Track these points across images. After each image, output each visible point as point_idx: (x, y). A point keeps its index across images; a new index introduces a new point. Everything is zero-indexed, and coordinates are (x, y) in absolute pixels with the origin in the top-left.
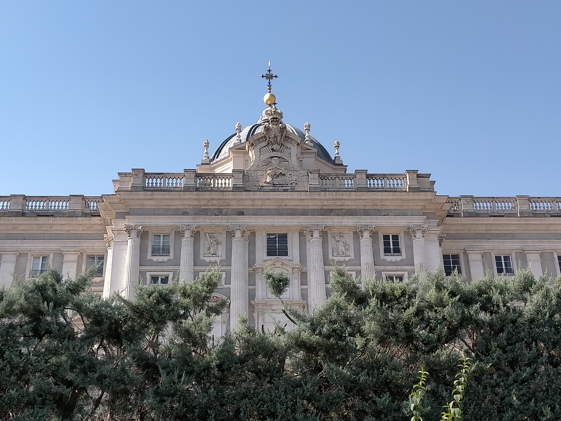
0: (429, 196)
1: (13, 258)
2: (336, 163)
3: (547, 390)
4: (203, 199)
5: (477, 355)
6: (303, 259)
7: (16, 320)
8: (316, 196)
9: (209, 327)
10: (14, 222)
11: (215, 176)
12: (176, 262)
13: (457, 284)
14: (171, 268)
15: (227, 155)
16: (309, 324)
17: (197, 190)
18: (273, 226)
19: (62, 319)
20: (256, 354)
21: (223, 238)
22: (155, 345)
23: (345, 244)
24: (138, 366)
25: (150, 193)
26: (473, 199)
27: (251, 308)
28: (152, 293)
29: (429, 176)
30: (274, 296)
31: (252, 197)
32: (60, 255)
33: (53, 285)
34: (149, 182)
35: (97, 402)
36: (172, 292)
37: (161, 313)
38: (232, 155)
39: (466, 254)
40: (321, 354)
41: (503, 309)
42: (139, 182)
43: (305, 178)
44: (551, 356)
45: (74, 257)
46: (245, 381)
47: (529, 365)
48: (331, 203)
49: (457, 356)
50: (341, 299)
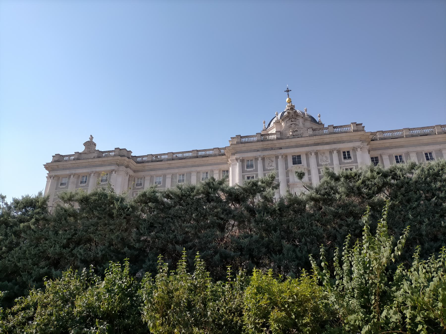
0: (362, 133)
1: (195, 174)
2: (319, 123)
3: (426, 211)
4: (265, 144)
6: (308, 165)
7: (201, 196)
8: (312, 138)
9: (274, 194)
10: (194, 160)
11: (269, 135)
13: (380, 169)
14: (254, 173)
15: (273, 126)
16: (315, 190)
17: (262, 141)
18: (294, 153)
19: (217, 195)
20: (294, 204)
22: (253, 203)
23: (326, 157)
24: (247, 211)
25: (243, 144)
26: (383, 132)
29: (361, 124)
30: (299, 180)
31: (284, 142)
33: (212, 182)
34: (243, 140)
35: (233, 226)
38: (275, 125)
40: (321, 202)
41: (402, 178)
42: (239, 140)
44: (426, 197)
45: (217, 172)
46: (290, 215)
47: (416, 201)
49: (382, 199)
50: (328, 179)
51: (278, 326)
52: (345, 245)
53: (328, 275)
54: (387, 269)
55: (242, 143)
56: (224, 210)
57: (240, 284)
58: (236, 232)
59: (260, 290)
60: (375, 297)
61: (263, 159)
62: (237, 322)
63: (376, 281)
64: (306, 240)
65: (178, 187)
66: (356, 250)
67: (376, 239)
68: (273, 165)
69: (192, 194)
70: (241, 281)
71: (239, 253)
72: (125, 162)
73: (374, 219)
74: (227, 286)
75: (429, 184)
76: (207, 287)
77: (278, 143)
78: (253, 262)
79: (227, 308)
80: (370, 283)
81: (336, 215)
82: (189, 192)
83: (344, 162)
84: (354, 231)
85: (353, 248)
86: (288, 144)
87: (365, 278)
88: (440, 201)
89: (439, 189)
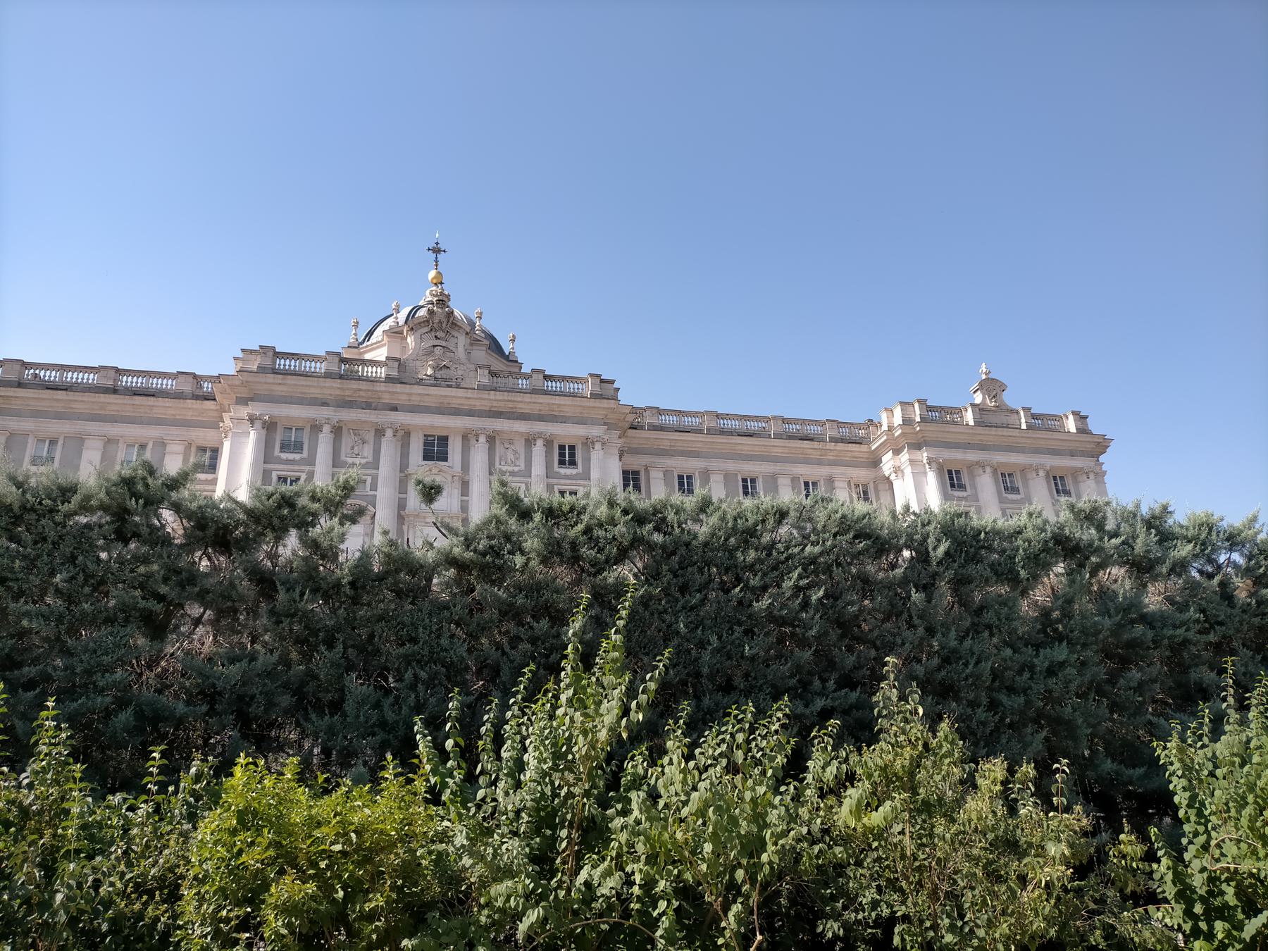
0: (612, 404)
2: (510, 359)
4: (348, 389)
5: (646, 578)
6: (465, 466)
7: (95, 519)
8: (485, 395)
9: (342, 538)
11: (364, 363)
12: (311, 461)
15: (380, 339)
16: (462, 539)
17: (341, 377)
18: (432, 427)
19: (156, 522)
20: (397, 571)
21: (370, 437)
22: (273, 556)
23: (515, 452)
24: (250, 580)
25: (280, 376)
27: (401, 519)
28: (273, 494)
29: (613, 382)
30: (423, 506)
31: (407, 391)
32: (162, 444)
33: (144, 479)
35: (197, 622)
36: (298, 494)
37: (282, 518)
38: (386, 339)
39: (647, 470)
40: (475, 573)
41: (677, 531)
43: (472, 374)
46: (383, 601)
47: (699, 591)
48: (502, 404)
49: (625, 579)
51: (288, 926)
52: (518, 692)
53: (459, 775)
54: (608, 761)
56: (172, 572)
57: (188, 804)
58: (204, 640)
59: (247, 819)
60: (570, 834)
61: (337, 431)
63: (577, 790)
64: (415, 676)
66: (541, 706)
67: (594, 679)
69: (64, 508)
70: (193, 793)
71: (205, 708)
74: (144, 809)
75: (731, 553)
76: (67, 812)
77: (389, 392)
78: (245, 737)
80: (563, 794)
81: (509, 612)
82: (54, 500)
83: (558, 473)
84: (547, 656)
85: (535, 702)
86: (415, 400)
87: (552, 783)
88: (749, 594)
89: (751, 567)
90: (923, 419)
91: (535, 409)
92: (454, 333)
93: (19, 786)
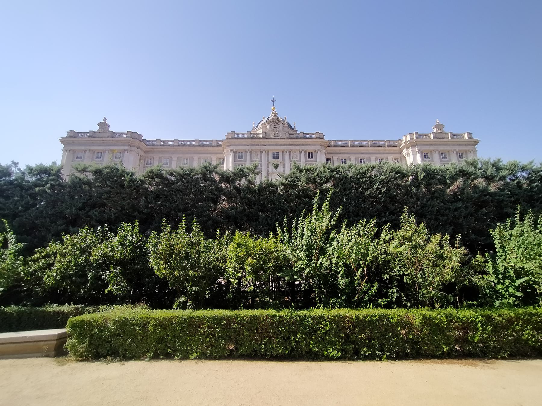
5: (334, 187)
6: (283, 160)
7: (199, 176)
8: (288, 140)
11: (257, 134)
17: (251, 138)
19: (212, 176)
21: (259, 153)
22: (239, 184)
23: (296, 155)
33: (209, 166)
34: (236, 136)
35: (224, 200)
36: (244, 168)
37: (241, 174)
41: (343, 174)
42: (233, 136)
43: (284, 134)
47: (349, 190)
48: (292, 142)
50: (295, 170)
52: (301, 217)
53: (287, 237)
54: (325, 233)
55: (235, 138)
56: (217, 188)
57: (226, 242)
58: (225, 204)
60: (316, 251)
61: (251, 152)
62: (222, 266)
63: (317, 241)
64: (275, 213)
65: (180, 168)
66: (308, 219)
67: (321, 213)
68: (258, 158)
69: (192, 174)
70: (227, 239)
71: (227, 220)
72: (137, 144)
73: (322, 200)
74: (216, 243)
75: (358, 179)
76: (201, 243)
78: (237, 227)
79: (215, 257)
80: (314, 242)
81: (298, 196)
82: (190, 172)
84: (308, 208)
85: (306, 219)
87: (311, 239)
88: (364, 190)
89: (364, 183)
90: (416, 138)
91: (301, 143)
92: (279, 124)
93: (190, 237)
